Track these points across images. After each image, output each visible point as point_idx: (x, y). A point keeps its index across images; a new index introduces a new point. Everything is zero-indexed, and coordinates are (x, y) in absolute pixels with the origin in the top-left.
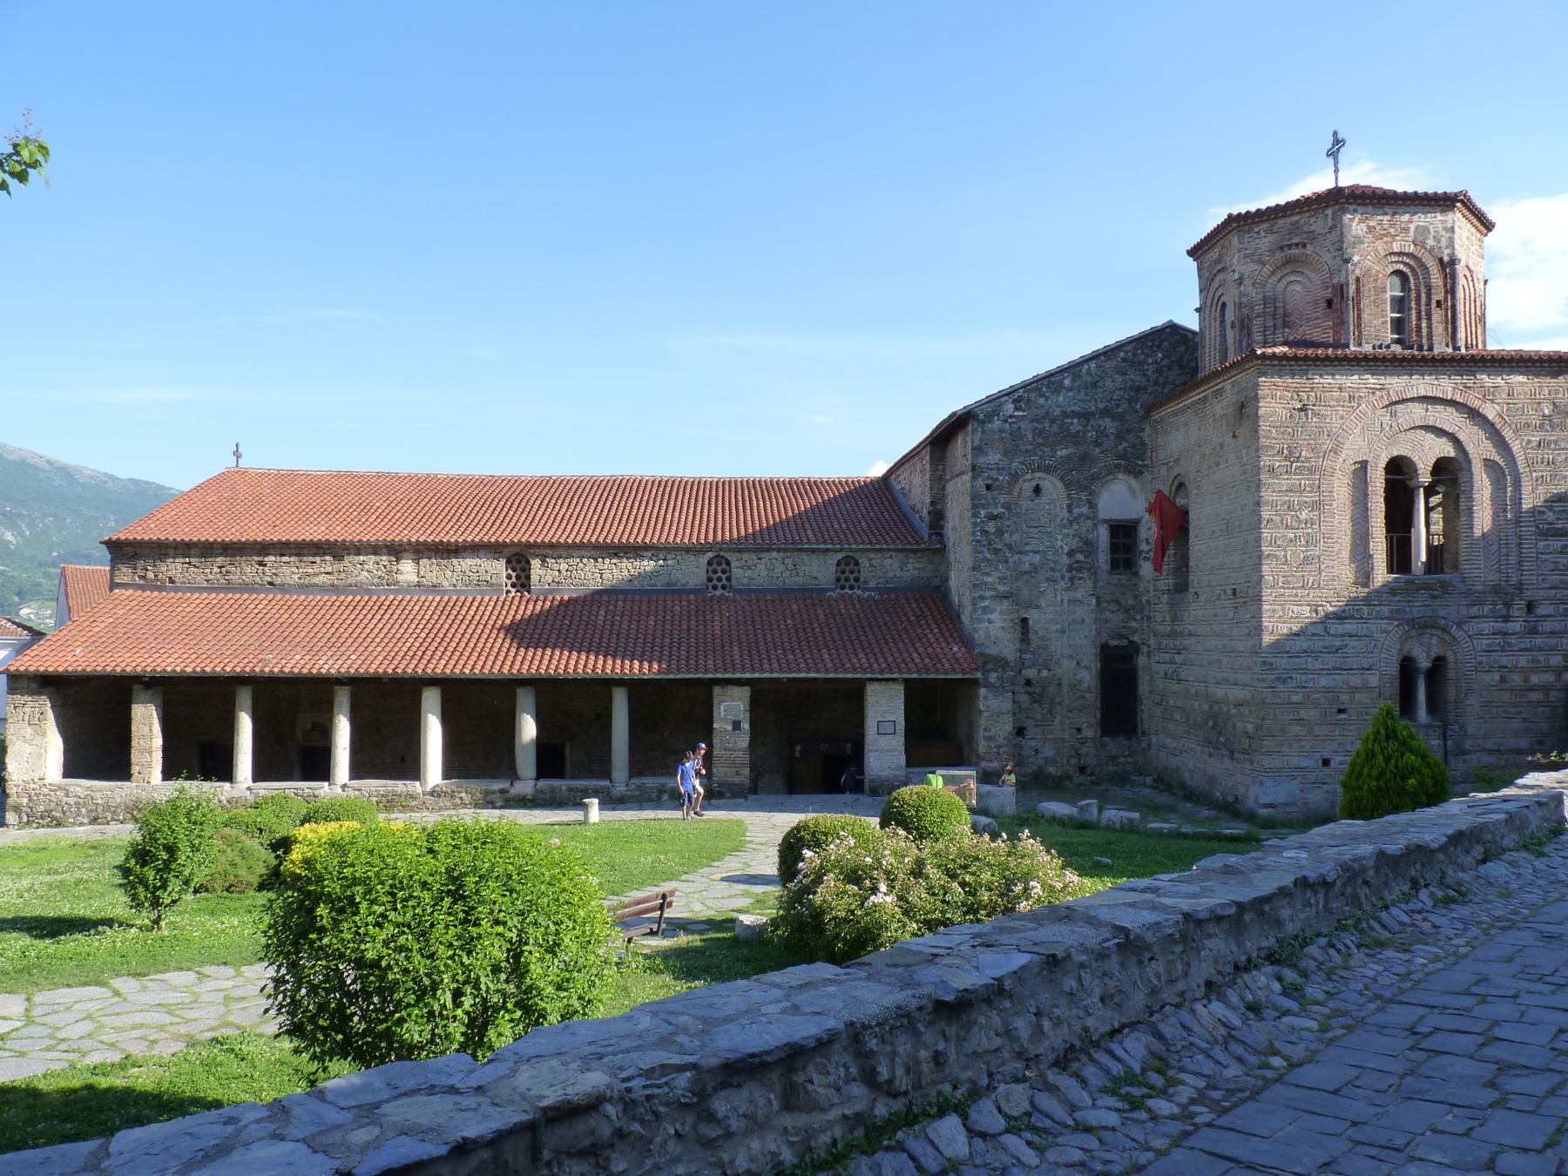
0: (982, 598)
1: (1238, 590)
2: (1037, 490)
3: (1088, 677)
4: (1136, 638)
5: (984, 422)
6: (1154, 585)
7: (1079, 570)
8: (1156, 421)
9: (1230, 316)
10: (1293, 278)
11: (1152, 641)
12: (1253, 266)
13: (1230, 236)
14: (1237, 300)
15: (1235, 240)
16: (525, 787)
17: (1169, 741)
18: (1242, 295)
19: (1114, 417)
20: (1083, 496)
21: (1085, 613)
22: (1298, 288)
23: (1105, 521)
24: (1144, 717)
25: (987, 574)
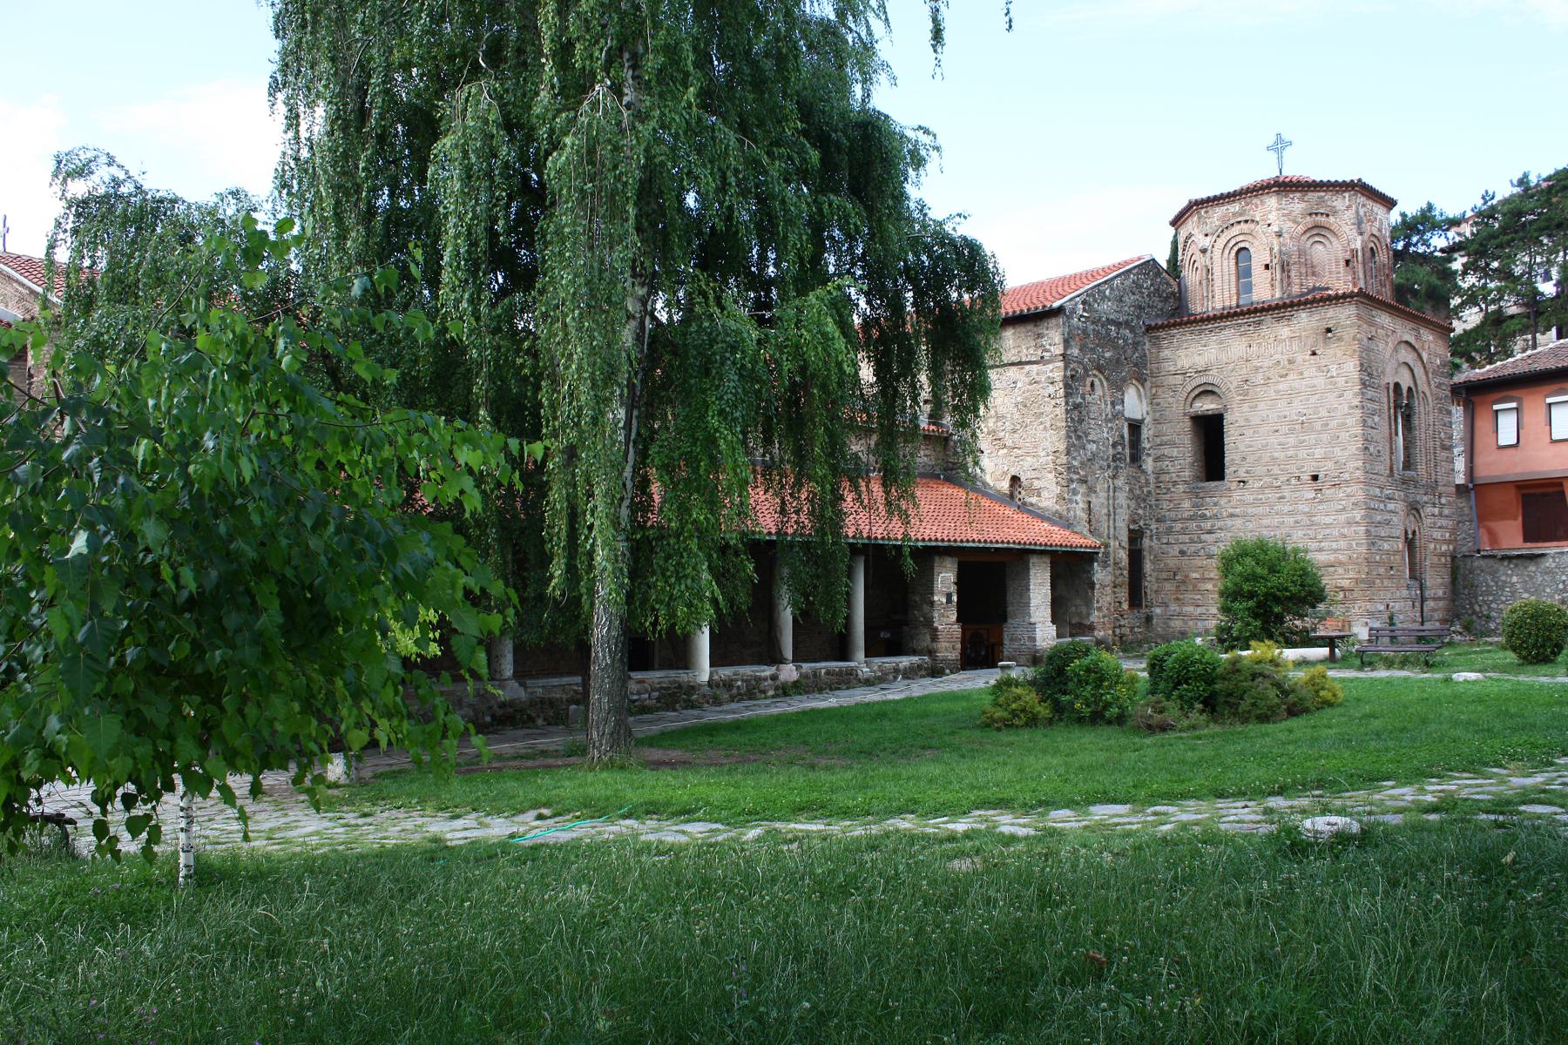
0: (1072, 481)
1: (1321, 476)
2: (1092, 385)
3: (1123, 556)
4: (1141, 523)
5: (1068, 317)
6: (1157, 478)
7: (1120, 459)
8: (1158, 338)
9: (1259, 257)
10: (1317, 239)
11: (1153, 527)
12: (1290, 224)
13: (1263, 198)
14: (1276, 249)
15: (1272, 201)
16: (789, 672)
17: (1190, 609)
18: (1281, 245)
19: (1132, 330)
20: (1119, 395)
21: (1122, 498)
22: (1320, 247)
23: (1127, 419)
24: (1148, 591)
25: (1074, 458)
